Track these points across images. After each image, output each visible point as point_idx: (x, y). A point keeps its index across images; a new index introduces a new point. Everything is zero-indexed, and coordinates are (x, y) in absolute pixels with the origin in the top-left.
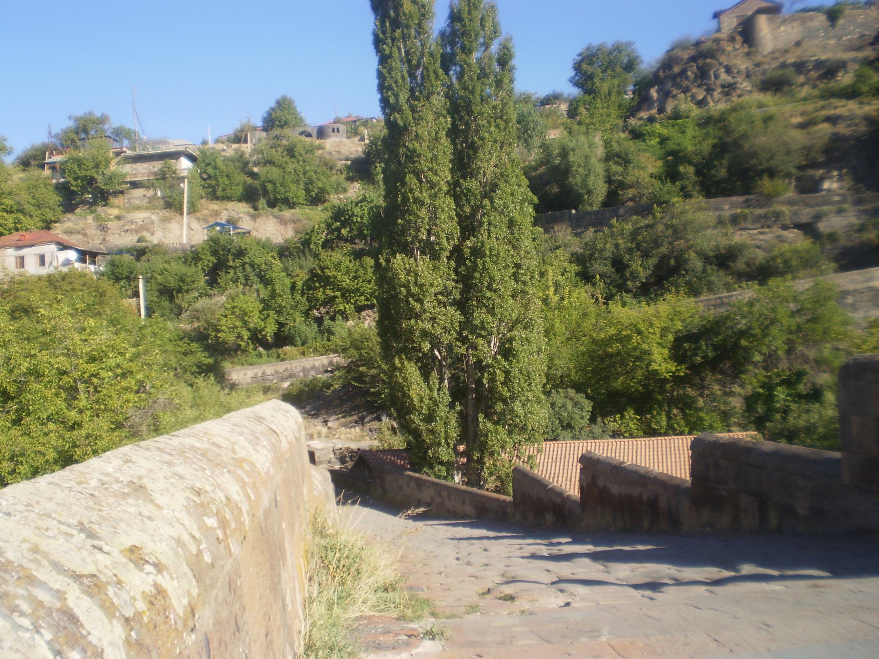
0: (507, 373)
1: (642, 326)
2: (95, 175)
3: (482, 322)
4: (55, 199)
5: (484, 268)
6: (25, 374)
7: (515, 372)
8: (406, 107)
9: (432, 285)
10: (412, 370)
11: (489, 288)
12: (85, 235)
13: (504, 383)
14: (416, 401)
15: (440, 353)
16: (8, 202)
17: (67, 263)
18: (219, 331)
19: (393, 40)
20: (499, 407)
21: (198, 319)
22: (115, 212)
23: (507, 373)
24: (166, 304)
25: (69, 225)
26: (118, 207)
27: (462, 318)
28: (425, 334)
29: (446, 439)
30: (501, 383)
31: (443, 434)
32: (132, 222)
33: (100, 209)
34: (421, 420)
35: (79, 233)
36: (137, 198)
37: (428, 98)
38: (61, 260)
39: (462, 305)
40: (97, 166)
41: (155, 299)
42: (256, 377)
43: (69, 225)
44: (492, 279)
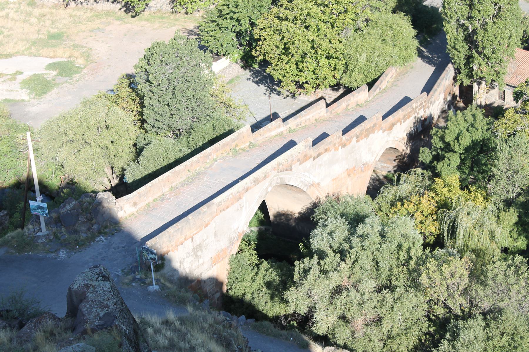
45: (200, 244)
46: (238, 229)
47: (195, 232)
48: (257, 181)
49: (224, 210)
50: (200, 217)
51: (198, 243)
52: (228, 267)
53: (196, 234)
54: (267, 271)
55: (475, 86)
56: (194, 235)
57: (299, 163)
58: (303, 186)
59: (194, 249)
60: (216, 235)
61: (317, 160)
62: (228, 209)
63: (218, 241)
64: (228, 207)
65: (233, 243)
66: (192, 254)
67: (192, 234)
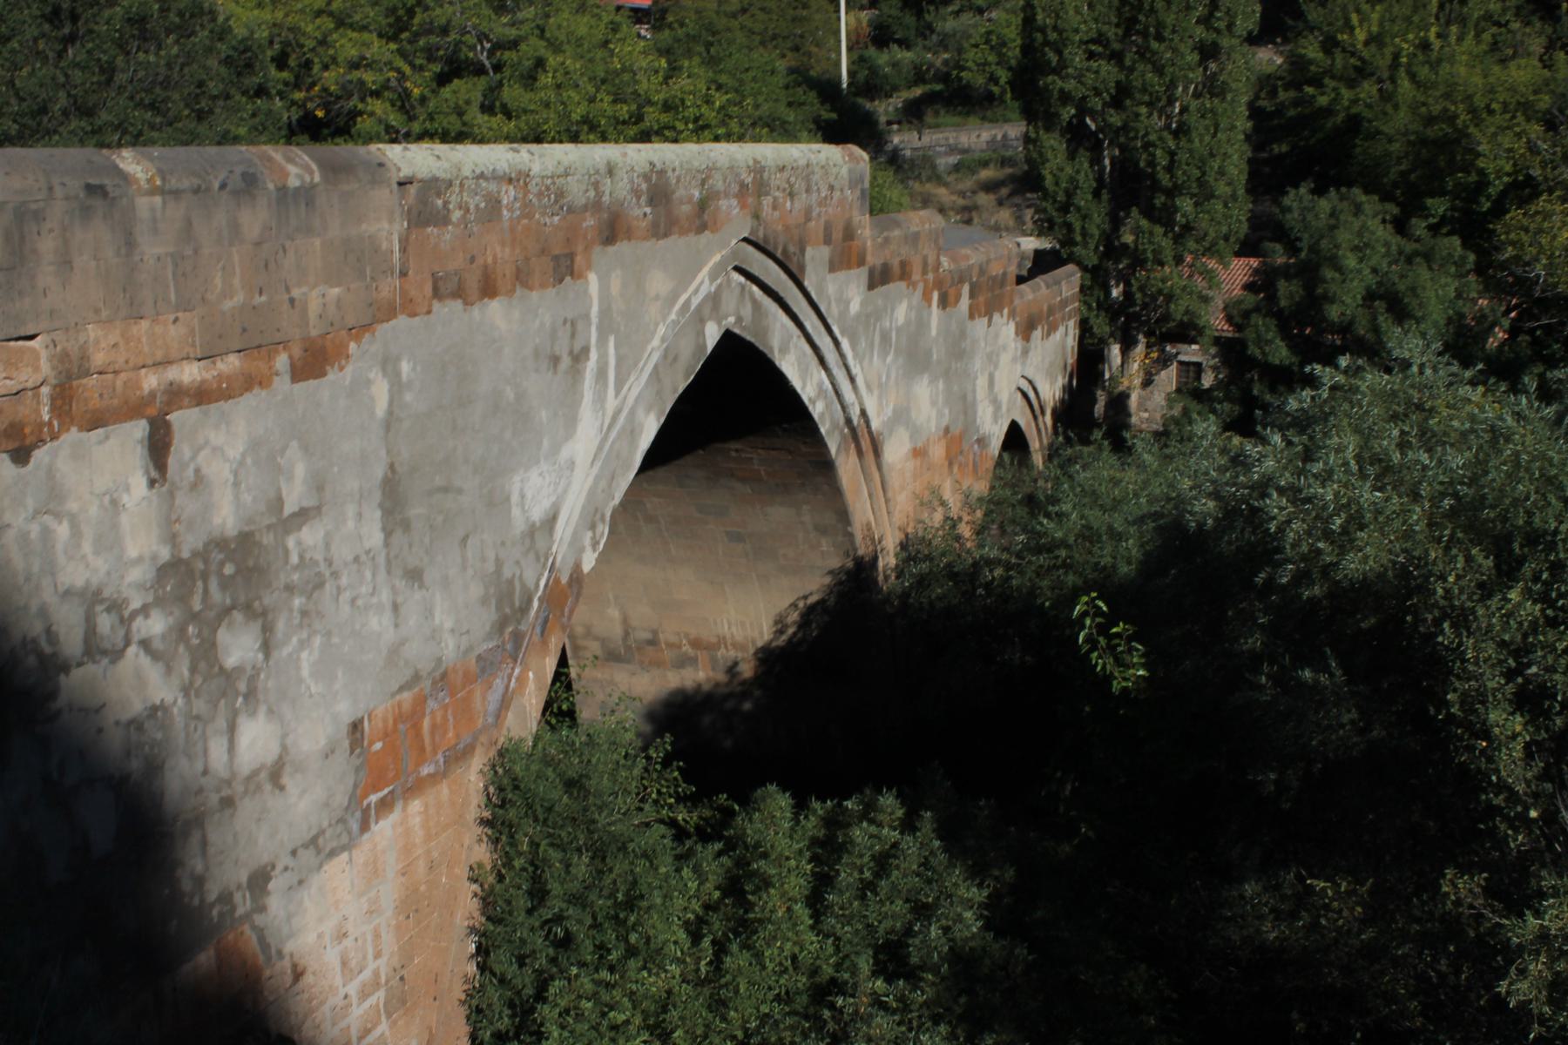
0: (1172, 154)
1: (1479, 101)
3: (1144, 84)
6: (578, 123)
7: (1183, 156)
9: (1077, 31)
10: (1055, 145)
11: (1159, 38)
13: (1169, 169)
14: (1049, 181)
15: (1093, 119)
18: (963, 69)
20: (1160, 200)
21: (946, 49)
23: (1172, 154)
24: (910, 19)
28: (1065, 97)
29: (1084, 234)
31: (1078, 229)
34: (1058, 210)
41: (894, 12)
42: (993, 140)
44: (1160, 25)
45: (246, 540)
46: (551, 520)
47: (190, 373)
49: (459, 293)
50: (254, 219)
51: (226, 517)
52: (482, 853)
53: (202, 396)
54: (828, 850)
55: (1115, 350)
56: (176, 395)
59: (177, 575)
62: (495, 307)
63: (415, 576)
64: (489, 289)
65: (518, 637)
66: (155, 625)
67: (151, 381)
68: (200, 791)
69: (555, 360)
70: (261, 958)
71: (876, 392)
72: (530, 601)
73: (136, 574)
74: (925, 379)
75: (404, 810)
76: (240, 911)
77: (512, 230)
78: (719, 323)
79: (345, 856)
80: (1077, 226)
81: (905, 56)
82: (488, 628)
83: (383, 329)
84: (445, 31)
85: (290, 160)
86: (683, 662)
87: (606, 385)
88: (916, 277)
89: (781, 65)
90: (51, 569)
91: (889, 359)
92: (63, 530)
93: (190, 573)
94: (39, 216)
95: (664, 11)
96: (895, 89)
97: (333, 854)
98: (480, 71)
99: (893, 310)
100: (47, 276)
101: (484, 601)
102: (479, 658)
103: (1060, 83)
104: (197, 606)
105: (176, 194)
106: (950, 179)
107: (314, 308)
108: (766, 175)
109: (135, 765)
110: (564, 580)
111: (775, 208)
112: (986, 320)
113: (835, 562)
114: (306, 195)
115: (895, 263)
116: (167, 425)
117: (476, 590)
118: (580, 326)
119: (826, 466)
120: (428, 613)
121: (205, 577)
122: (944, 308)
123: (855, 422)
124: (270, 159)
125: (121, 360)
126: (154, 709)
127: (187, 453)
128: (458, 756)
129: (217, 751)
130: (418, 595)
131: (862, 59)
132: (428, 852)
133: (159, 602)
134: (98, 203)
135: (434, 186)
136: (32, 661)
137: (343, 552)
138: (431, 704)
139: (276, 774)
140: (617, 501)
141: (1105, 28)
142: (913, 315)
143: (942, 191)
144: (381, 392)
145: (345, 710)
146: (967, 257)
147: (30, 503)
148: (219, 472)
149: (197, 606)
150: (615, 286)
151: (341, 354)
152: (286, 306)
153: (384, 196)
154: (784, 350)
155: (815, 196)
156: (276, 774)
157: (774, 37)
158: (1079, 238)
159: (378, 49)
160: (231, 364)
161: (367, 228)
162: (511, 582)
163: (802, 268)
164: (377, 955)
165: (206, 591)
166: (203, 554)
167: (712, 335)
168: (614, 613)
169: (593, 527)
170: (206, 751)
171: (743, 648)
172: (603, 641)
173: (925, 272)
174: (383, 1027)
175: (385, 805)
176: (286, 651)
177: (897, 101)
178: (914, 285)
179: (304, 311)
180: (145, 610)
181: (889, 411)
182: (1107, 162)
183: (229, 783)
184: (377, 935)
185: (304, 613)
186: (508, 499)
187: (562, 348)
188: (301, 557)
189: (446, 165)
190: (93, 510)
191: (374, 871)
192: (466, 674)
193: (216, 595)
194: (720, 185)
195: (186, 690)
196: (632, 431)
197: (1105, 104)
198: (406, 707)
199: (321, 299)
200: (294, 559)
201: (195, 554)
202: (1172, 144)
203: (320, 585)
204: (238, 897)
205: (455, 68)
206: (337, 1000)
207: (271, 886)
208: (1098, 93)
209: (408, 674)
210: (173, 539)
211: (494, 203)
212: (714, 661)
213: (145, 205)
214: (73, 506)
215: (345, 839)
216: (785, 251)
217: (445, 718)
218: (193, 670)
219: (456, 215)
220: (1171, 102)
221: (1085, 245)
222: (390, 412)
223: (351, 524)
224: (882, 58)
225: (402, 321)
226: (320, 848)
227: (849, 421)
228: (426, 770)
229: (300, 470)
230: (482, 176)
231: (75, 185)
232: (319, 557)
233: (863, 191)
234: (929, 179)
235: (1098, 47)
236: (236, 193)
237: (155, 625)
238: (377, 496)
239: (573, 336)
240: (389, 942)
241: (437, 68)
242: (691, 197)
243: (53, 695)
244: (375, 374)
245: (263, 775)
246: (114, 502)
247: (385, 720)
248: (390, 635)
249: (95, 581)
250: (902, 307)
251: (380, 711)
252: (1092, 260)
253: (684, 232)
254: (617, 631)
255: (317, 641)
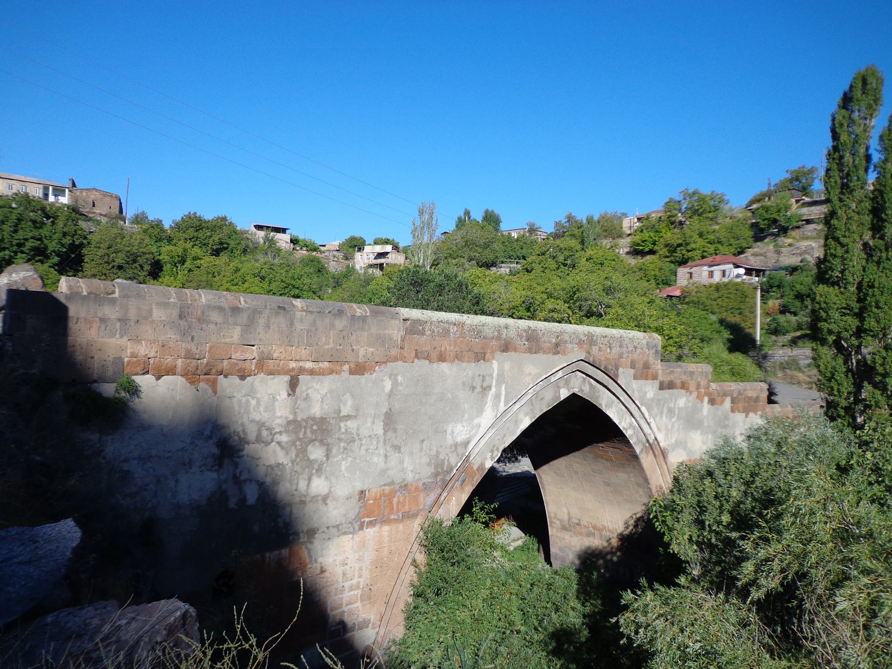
2: (777, 217)
4: (749, 233)
5: (873, 295)
8: (835, 199)
9: (835, 304)
10: (827, 353)
11: (878, 307)
12: (765, 257)
13: (882, 365)
14: (822, 367)
16: (711, 237)
17: (738, 276)
19: (834, 159)
20: (878, 379)
22: (789, 241)
24: (798, 303)
25: (756, 250)
26: (793, 238)
27: (858, 324)
28: (830, 332)
29: (839, 391)
30: (881, 365)
32: (798, 248)
33: (782, 240)
35: (762, 255)
36: (810, 231)
37: (851, 192)
38: (735, 274)
39: (860, 316)
40: (779, 211)
43: (756, 250)
44: (877, 302)
45: (323, 420)
46: (466, 443)
47: (309, 365)
48: (533, 343)
49: (428, 358)
50: (340, 324)
51: (316, 410)
52: (421, 558)
53: (312, 372)
56: (302, 371)
57: (632, 371)
58: (635, 440)
59: (294, 425)
60: (389, 420)
61: (667, 393)
62: (444, 366)
63: (397, 448)
64: (442, 358)
67: (293, 365)
68: (293, 495)
69: (473, 388)
70: (308, 560)
71: (664, 432)
72: (452, 470)
73: (278, 421)
74: (699, 432)
75: (380, 528)
76: (302, 540)
77: (455, 341)
78: (569, 390)
79: (351, 536)
80: (835, 387)
81: (793, 319)
82: (429, 474)
83: (390, 365)
84: (586, 300)
85: (359, 308)
86: (590, 534)
87: (499, 401)
88: (692, 388)
89: (714, 318)
90: (248, 412)
91: (673, 420)
92: (253, 402)
93: (300, 426)
94: (260, 313)
95: (685, 297)
96: (788, 332)
97: (345, 533)
98: (600, 315)
99: (676, 400)
100: (260, 329)
101: (429, 464)
102: (424, 484)
103: (827, 325)
104: (301, 436)
105: (311, 312)
106: (805, 370)
107: (362, 352)
108: (595, 338)
109: (268, 480)
110: (475, 468)
111: (600, 351)
112: (744, 415)
113: (645, 500)
114: (363, 319)
115: (678, 382)
116: (298, 379)
117: (425, 460)
118: (487, 378)
119: (635, 457)
120: (402, 462)
121: (305, 428)
122: (712, 405)
123: (651, 442)
124: (352, 307)
125: (283, 357)
126: (279, 464)
127: (304, 388)
128: (409, 516)
129: (302, 485)
130: (397, 455)
131: (774, 319)
132: (390, 546)
133: (287, 432)
134: (282, 311)
135: (418, 322)
136: (236, 438)
137: (364, 432)
138: (398, 494)
139: (325, 499)
140: (507, 445)
141: (850, 303)
142: (690, 404)
143: (801, 374)
144: (388, 385)
145: (359, 486)
146: (730, 386)
147: (244, 392)
148: (316, 396)
149: (301, 436)
150: (507, 366)
151: (372, 370)
152: (350, 351)
153: (396, 323)
154: (609, 406)
155: (624, 350)
156: (325, 499)
157: (732, 309)
158: (836, 393)
159: (561, 306)
160: (326, 364)
161: (389, 332)
162: (443, 461)
163: (617, 376)
164: (360, 577)
165: (305, 433)
166: (306, 421)
167: (564, 394)
168: (565, 510)
169: (492, 452)
170: (297, 484)
171: (612, 532)
172: (561, 521)
173: (698, 387)
174: (358, 604)
175: (372, 524)
176: (335, 460)
177: (788, 337)
178: (691, 393)
179: (358, 353)
180: (280, 433)
181: (673, 440)
182: (854, 361)
183: (305, 496)
184: (361, 569)
185: (345, 449)
186: (445, 431)
187: (478, 383)
188: (346, 430)
189: (425, 316)
190: (266, 398)
191: (363, 545)
192: (417, 488)
193: (309, 434)
194: (567, 338)
195: (293, 462)
196: (517, 423)
197: (851, 336)
198: (387, 492)
199: (364, 352)
200: (343, 430)
201: (303, 420)
202: (884, 354)
203: (354, 441)
204: (301, 535)
205: (590, 314)
206: (339, 586)
207: (316, 536)
208: (847, 331)
209: (389, 481)
210: (295, 414)
211: (446, 333)
212: (601, 535)
213: (298, 314)
214: (259, 396)
215: (351, 530)
216: (606, 367)
217: (404, 500)
218: (297, 456)
219: (428, 333)
220: (885, 335)
221: (840, 396)
222: (391, 391)
223: (369, 424)
224: (782, 319)
225: (400, 363)
226: (339, 529)
227: (648, 441)
228: (392, 517)
229: (350, 403)
230: (441, 321)
231: (274, 306)
232: (354, 432)
233: (657, 351)
234: (795, 369)
235: (846, 310)
236: (335, 315)
237: (284, 438)
238: (382, 417)
239: (483, 381)
240: (366, 574)
241: (582, 314)
242: (550, 342)
243: (242, 450)
244: (387, 379)
245: (320, 498)
246: (274, 398)
247: (376, 494)
248: (382, 465)
249: (263, 420)
250: (682, 400)
251: (374, 490)
252: (844, 403)
253: (545, 353)
254: (566, 518)
255: (350, 459)
